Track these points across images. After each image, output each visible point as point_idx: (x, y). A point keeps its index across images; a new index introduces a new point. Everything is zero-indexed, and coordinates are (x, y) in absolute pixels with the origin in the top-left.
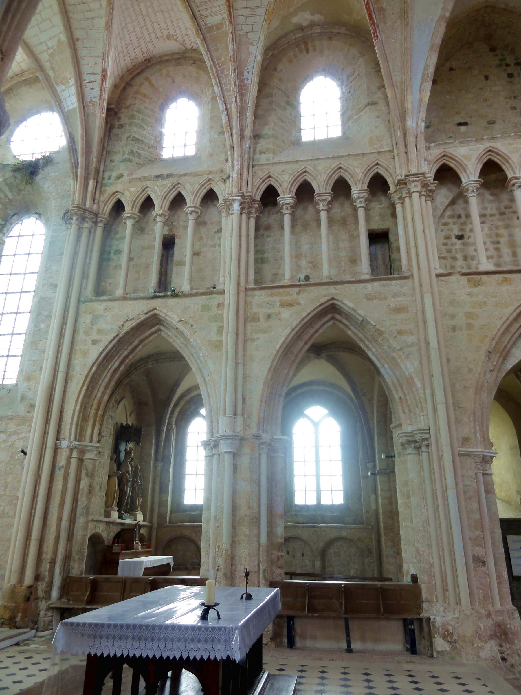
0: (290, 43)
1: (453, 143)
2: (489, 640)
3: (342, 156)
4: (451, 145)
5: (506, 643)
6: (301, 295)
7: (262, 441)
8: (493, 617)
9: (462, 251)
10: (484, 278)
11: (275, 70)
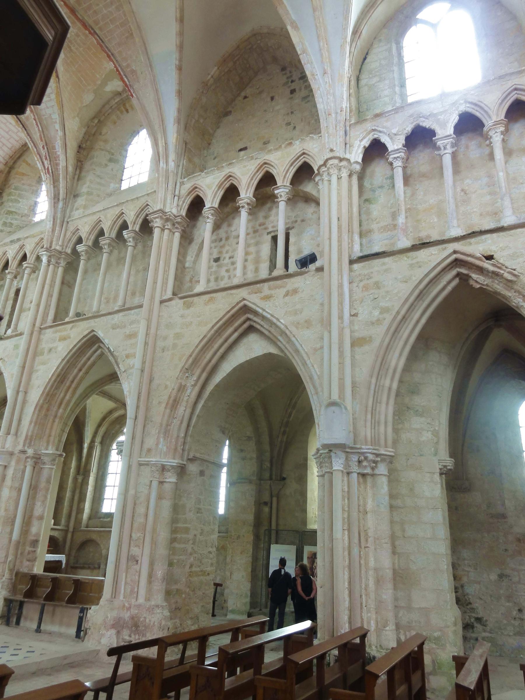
0: (113, 107)
1: (200, 175)
2: (111, 628)
3: (123, 203)
4: (199, 177)
5: (135, 634)
6: (73, 330)
7: (28, 455)
8: (132, 610)
9: (216, 272)
10: (196, 299)
11: (101, 134)
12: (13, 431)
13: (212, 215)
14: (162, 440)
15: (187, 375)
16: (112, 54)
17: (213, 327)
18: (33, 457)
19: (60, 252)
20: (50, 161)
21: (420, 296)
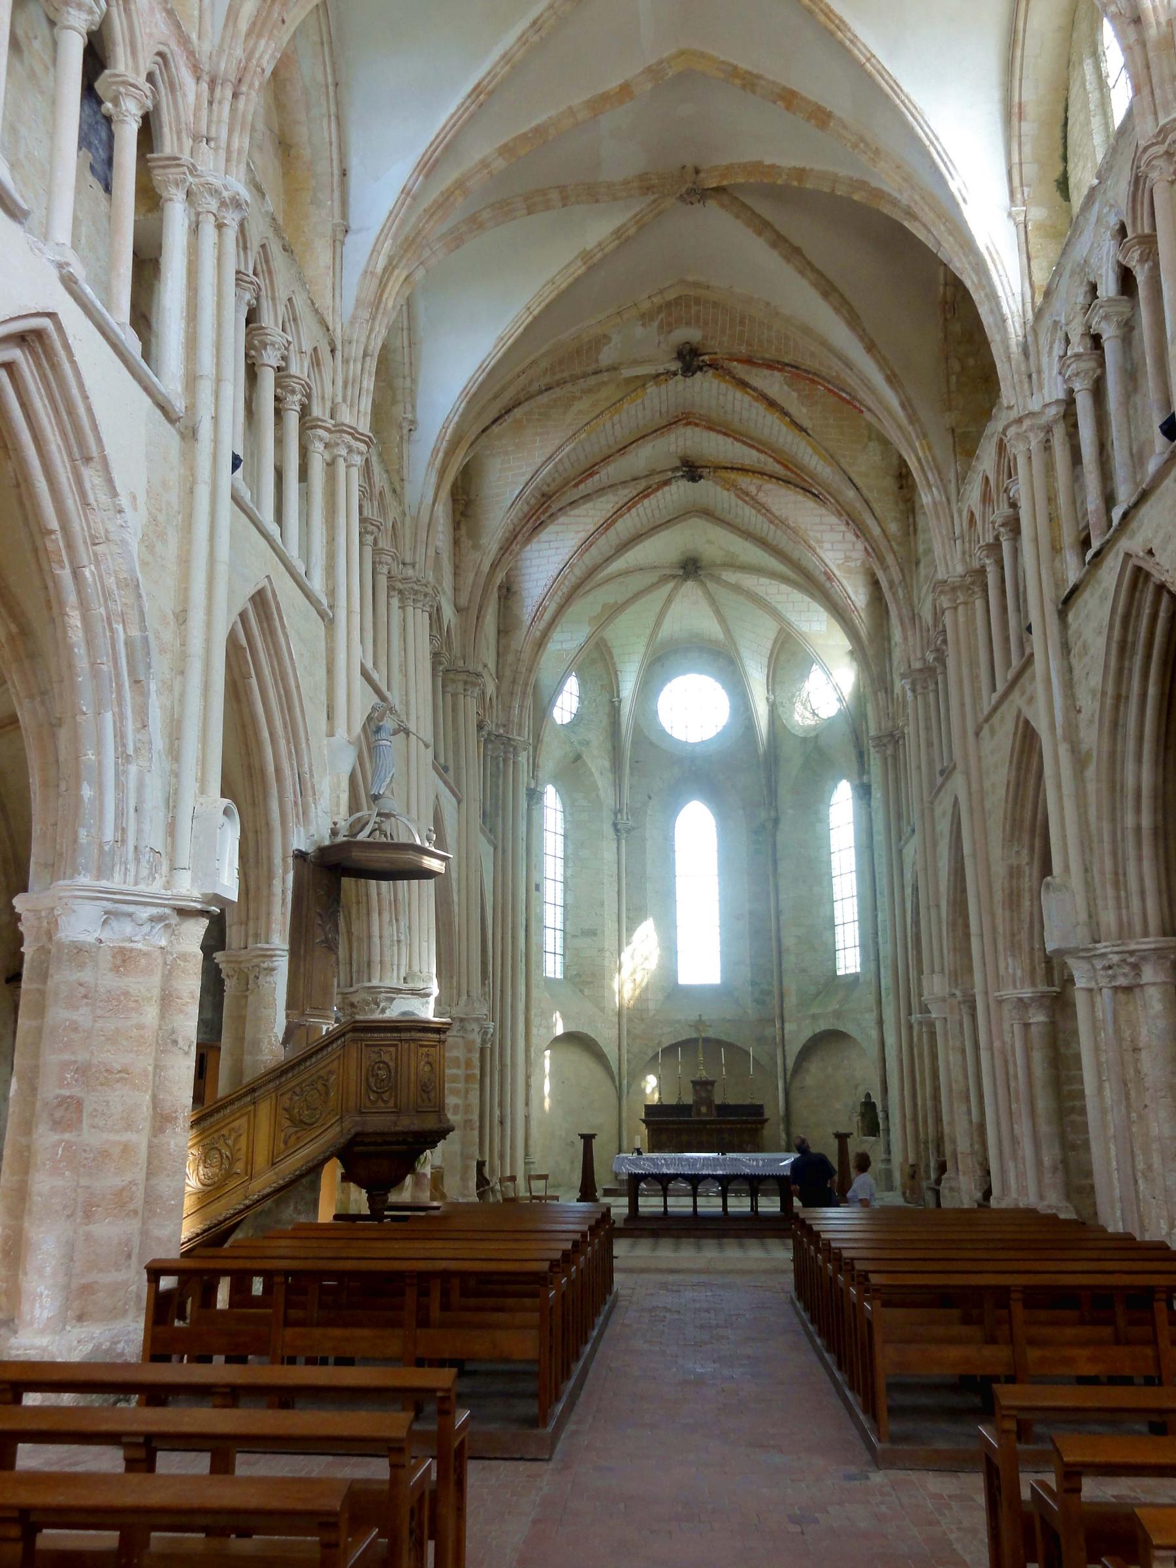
12: (937, 968)
13: (987, 557)
14: (1010, 960)
15: (1015, 849)
16: (815, 374)
17: (1011, 763)
18: (965, 1002)
19: (921, 670)
20: (864, 535)
21: (1124, 648)
